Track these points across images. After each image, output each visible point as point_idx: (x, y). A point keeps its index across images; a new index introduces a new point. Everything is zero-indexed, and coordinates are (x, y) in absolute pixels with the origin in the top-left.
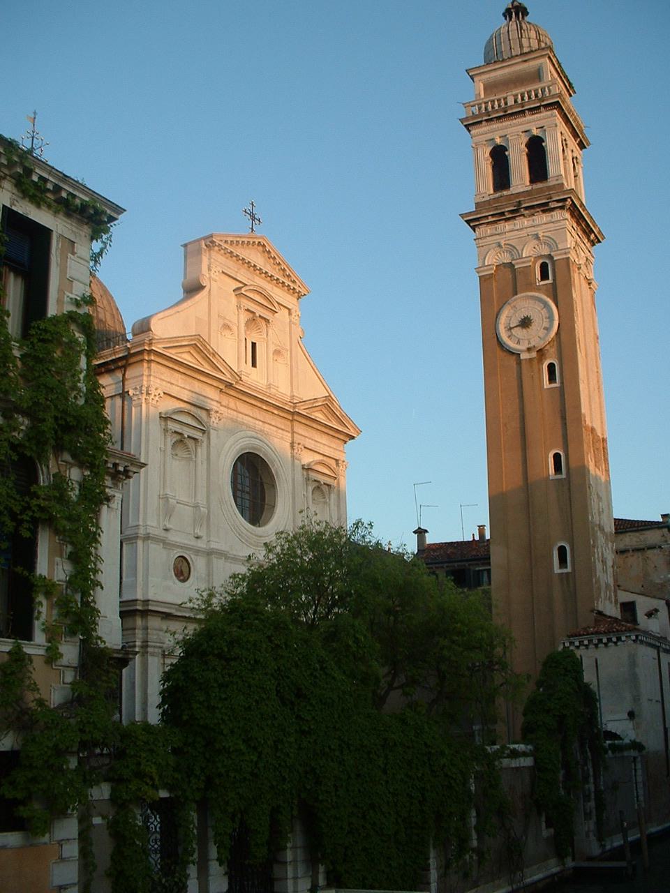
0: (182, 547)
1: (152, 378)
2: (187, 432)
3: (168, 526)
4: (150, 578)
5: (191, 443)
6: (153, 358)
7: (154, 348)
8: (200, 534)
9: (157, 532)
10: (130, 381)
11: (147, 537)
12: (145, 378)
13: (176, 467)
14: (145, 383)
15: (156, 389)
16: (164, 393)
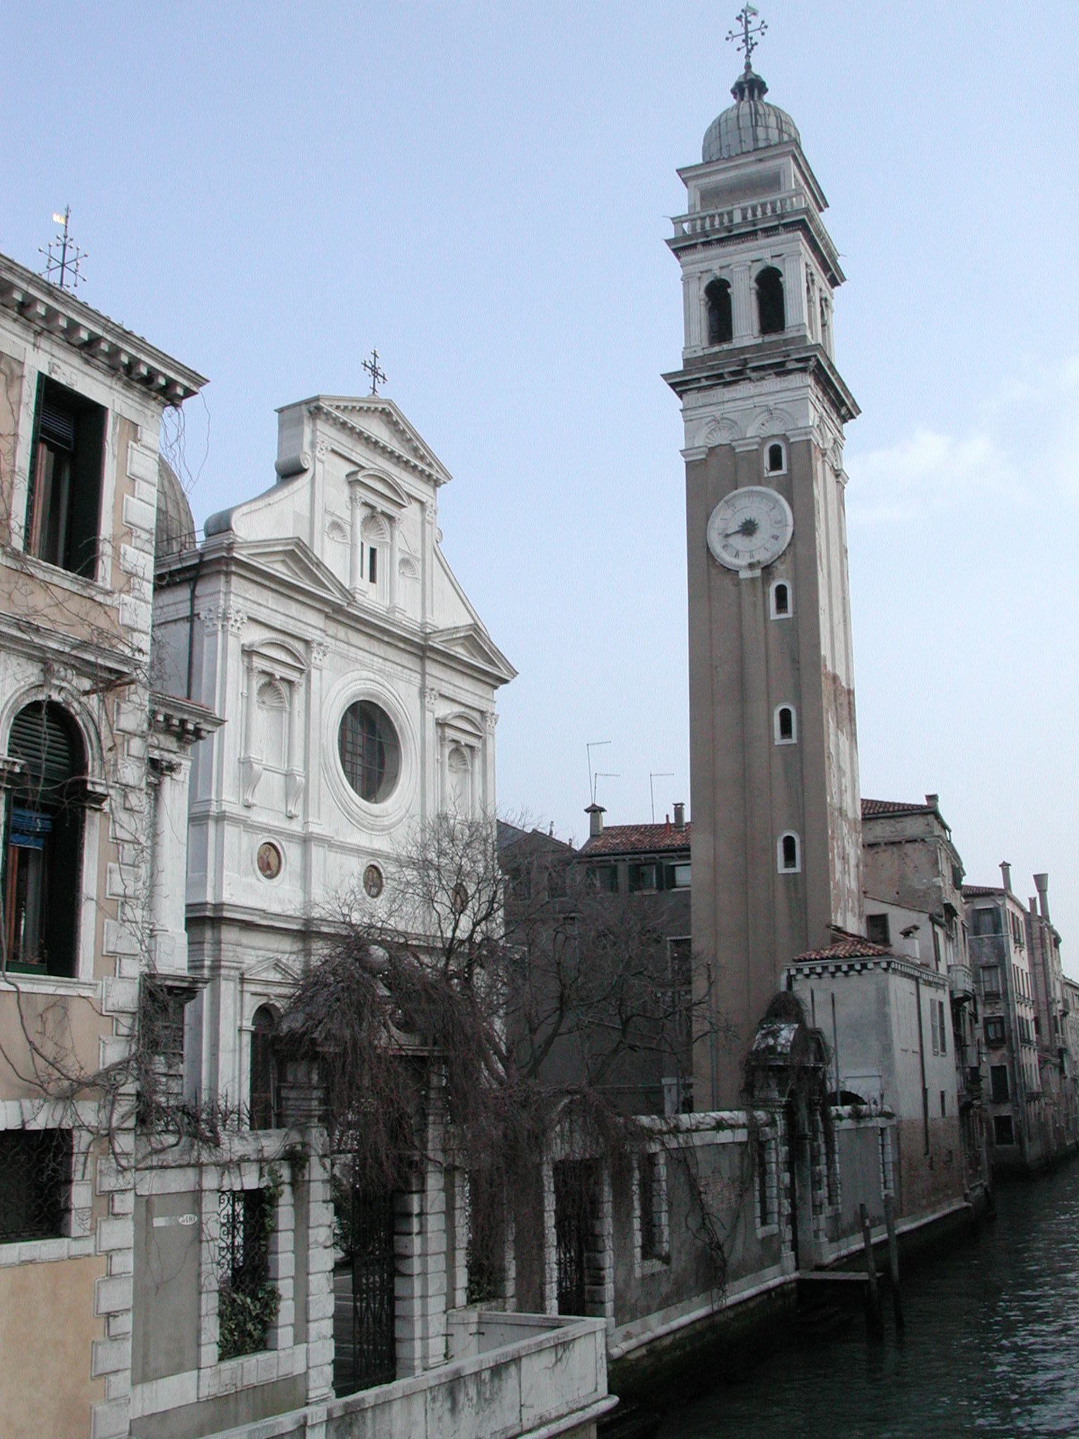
0: (269, 831)
2: (279, 672)
3: (251, 801)
4: (225, 872)
5: (284, 688)
6: (234, 568)
7: (235, 555)
12: (222, 596)
13: (262, 719)
14: (222, 602)
15: (238, 612)
16: (249, 618)
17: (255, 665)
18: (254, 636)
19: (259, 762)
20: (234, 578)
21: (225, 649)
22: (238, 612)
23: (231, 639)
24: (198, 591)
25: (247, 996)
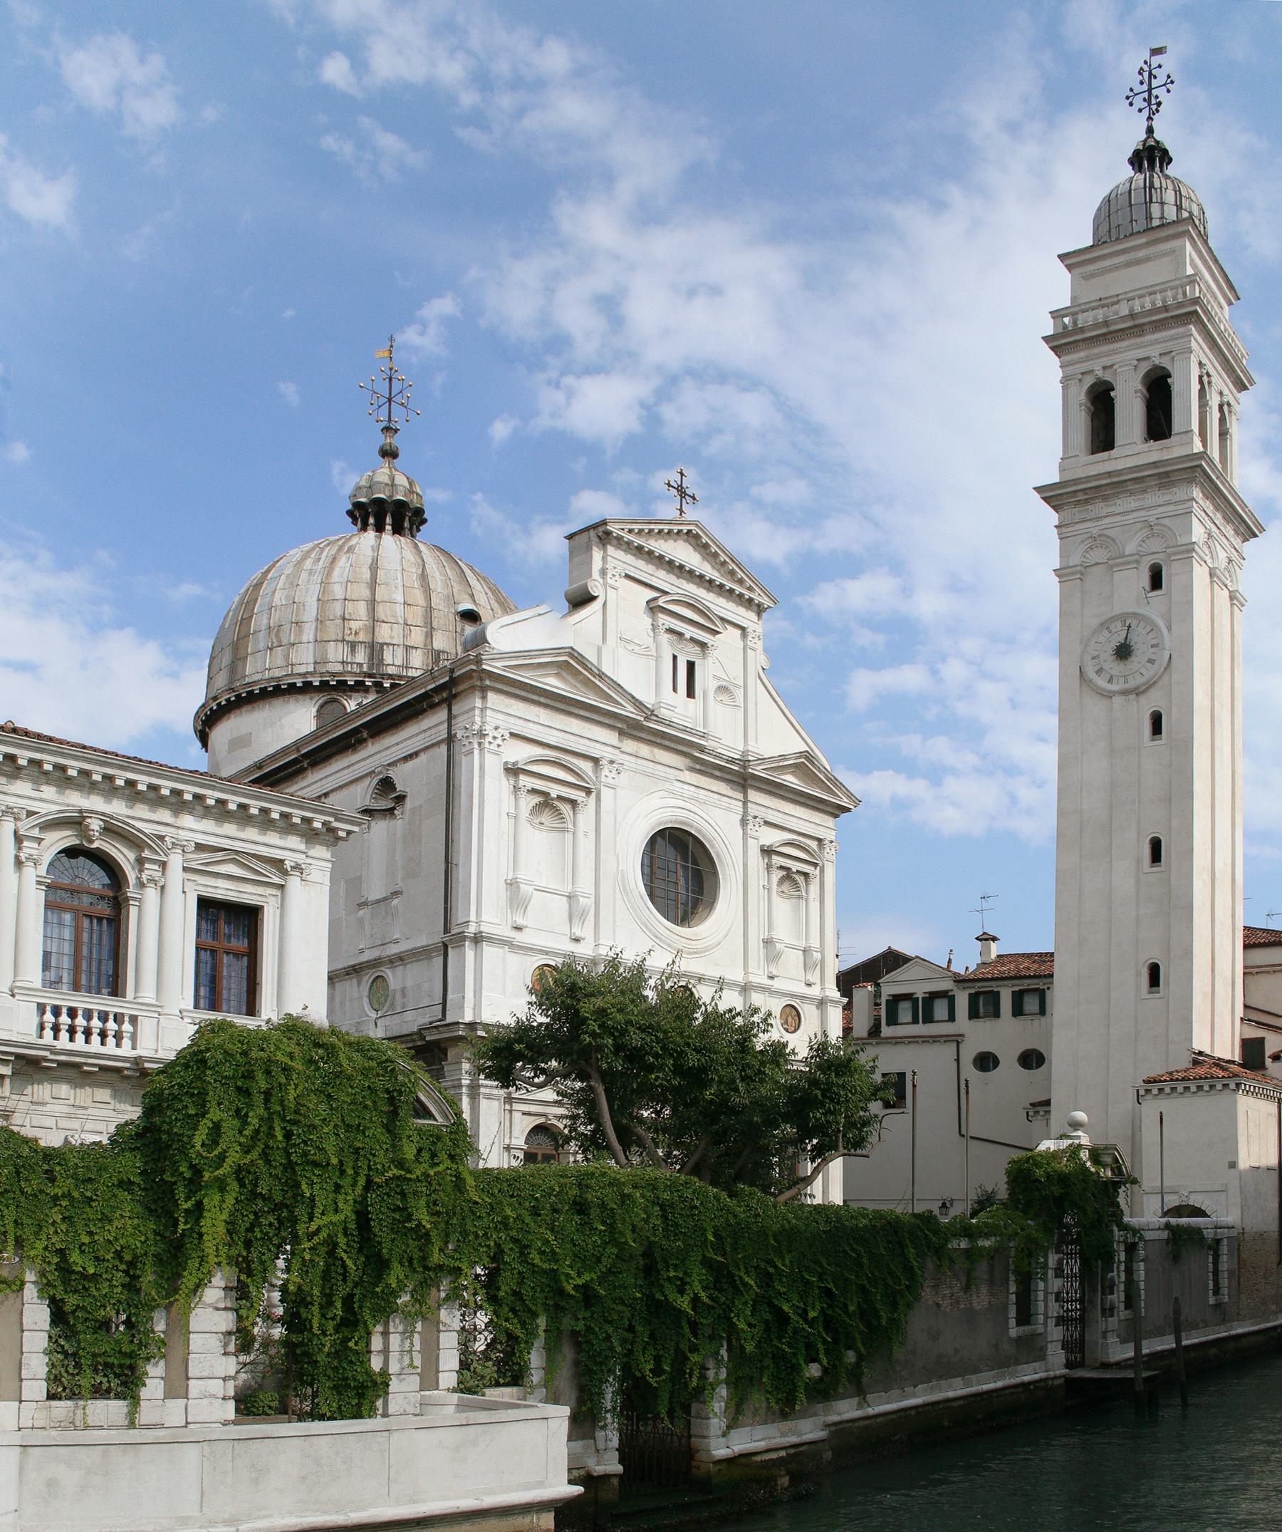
0: (547, 953)
1: (489, 712)
2: (555, 790)
4: (484, 993)
5: (565, 809)
6: (488, 682)
8: (578, 934)
9: (506, 932)
10: (459, 719)
11: (478, 939)
12: (477, 712)
13: (539, 841)
14: (478, 719)
15: (496, 728)
16: (512, 734)
17: (521, 783)
18: (520, 753)
19: (530, 883)
20: (490, 695)
21: (482, 767)
22: (496, 728)
23: (488, 756)
24: (455, 710)
25: (517, 1116)
